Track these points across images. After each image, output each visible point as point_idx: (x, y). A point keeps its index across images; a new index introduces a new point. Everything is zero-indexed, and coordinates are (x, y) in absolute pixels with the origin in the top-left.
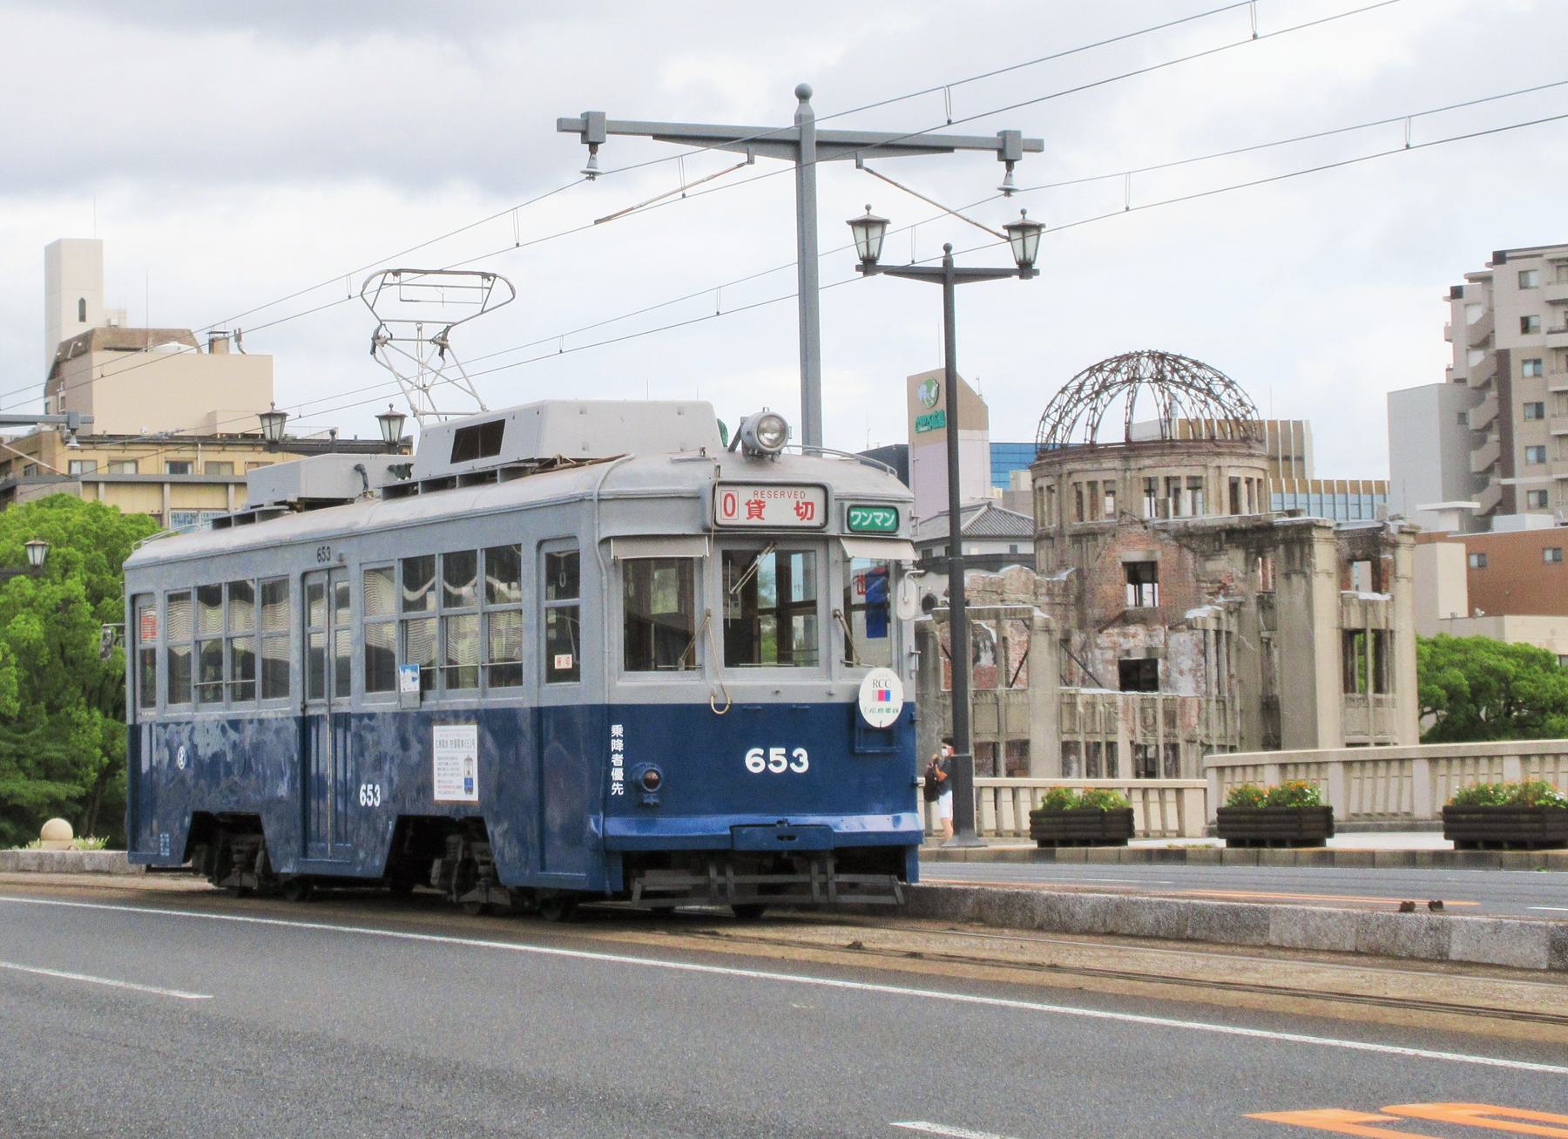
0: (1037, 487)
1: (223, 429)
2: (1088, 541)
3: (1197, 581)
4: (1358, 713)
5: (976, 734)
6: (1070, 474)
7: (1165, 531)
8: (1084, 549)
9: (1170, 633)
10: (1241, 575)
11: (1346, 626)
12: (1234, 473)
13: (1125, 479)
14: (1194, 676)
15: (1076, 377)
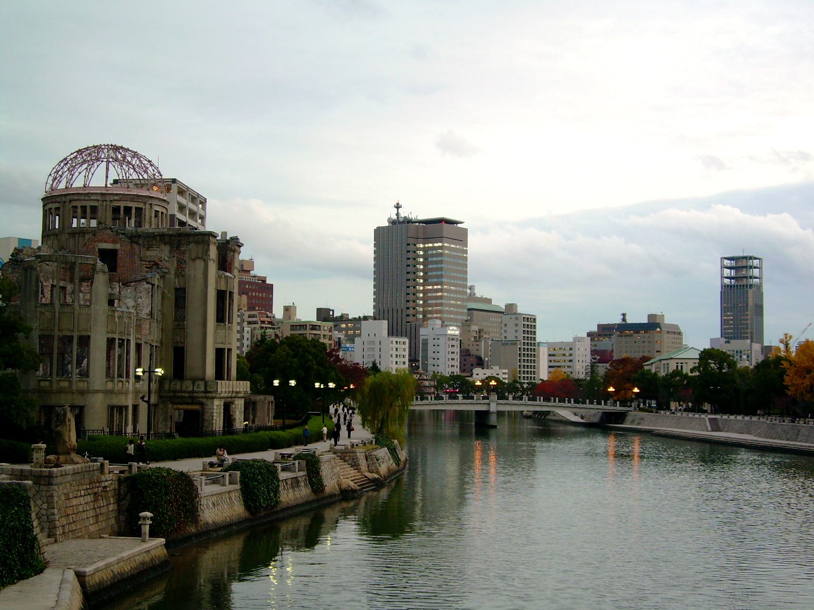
0: (47, 208)
2: (79, 236)
4: (221, 332)
5: (60, 330)
6: (70, 201)
7: (123, 234)
8: (77, 240)
9: (122, 286)
10: (167, 259)
11: (219, 289)
13: (102, 205)
14: (136, 309)
15: (72, 154)
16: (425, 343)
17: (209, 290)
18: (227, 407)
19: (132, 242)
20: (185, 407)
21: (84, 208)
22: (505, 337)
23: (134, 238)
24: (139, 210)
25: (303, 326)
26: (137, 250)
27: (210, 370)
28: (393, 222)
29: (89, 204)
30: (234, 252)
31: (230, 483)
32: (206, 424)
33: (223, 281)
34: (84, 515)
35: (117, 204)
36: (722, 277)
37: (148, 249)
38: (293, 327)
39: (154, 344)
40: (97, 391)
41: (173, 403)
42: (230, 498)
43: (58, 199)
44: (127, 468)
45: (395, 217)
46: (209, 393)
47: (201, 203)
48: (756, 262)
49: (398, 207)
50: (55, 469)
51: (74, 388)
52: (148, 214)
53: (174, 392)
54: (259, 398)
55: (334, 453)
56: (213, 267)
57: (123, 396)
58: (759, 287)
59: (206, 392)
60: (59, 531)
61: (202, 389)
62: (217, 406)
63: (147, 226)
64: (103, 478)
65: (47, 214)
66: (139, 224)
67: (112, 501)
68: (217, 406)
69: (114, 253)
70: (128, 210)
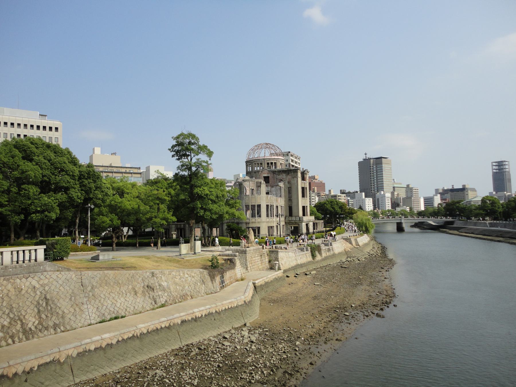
1: (113, 165)
3: (277, 179)
4: (304, 201)
6: (254, 162)
12: (281, 162)
16: (378, 200)
17: (299, 187)
18: (307, 225)
19: (274, 174)
20: (293, 225)
21: (258, 164)
22: (407, 196)
23: (274, 172)
24: (275, 163)
25: (335, 196)
26: (275, 176)
27: (301, 213)
28: (364, 160)
29: (259, 162)
30: (306, 174)
31: (306, 251)
32: (300, 231)
33: (303, 184)
34: (257, 263)
35: (268, 162)
36: (493, 169)
37: (279, 175)
38: (332, 196)
39: (282, 206)
40: (264, 222)
41: (289, 224)
42: (306, 256)
43: (250, 162)
44: (271, 247)
45: (365, 158)
46: (301, 220)
47: (299, 158)
48: (506, 163)
49: (366, 154)
50: (247, 249)
51: (257, 221)
52: (278, 164)
53: (289, 221)
54: (317, 221)
55: (344, 239)
56: (300, 179)
57: (272, 223)
58: (509, 172)
59: (300, 220)
60: (249, 269)
61: (298, 219)
62: (304, 225)
63: (278, 168)
64: (263, 250)
65: (247, 166)
66: (276, 168)
67: (267, 258)
68: (304, 225)
69: (268, 177)
70: (272, 163)
